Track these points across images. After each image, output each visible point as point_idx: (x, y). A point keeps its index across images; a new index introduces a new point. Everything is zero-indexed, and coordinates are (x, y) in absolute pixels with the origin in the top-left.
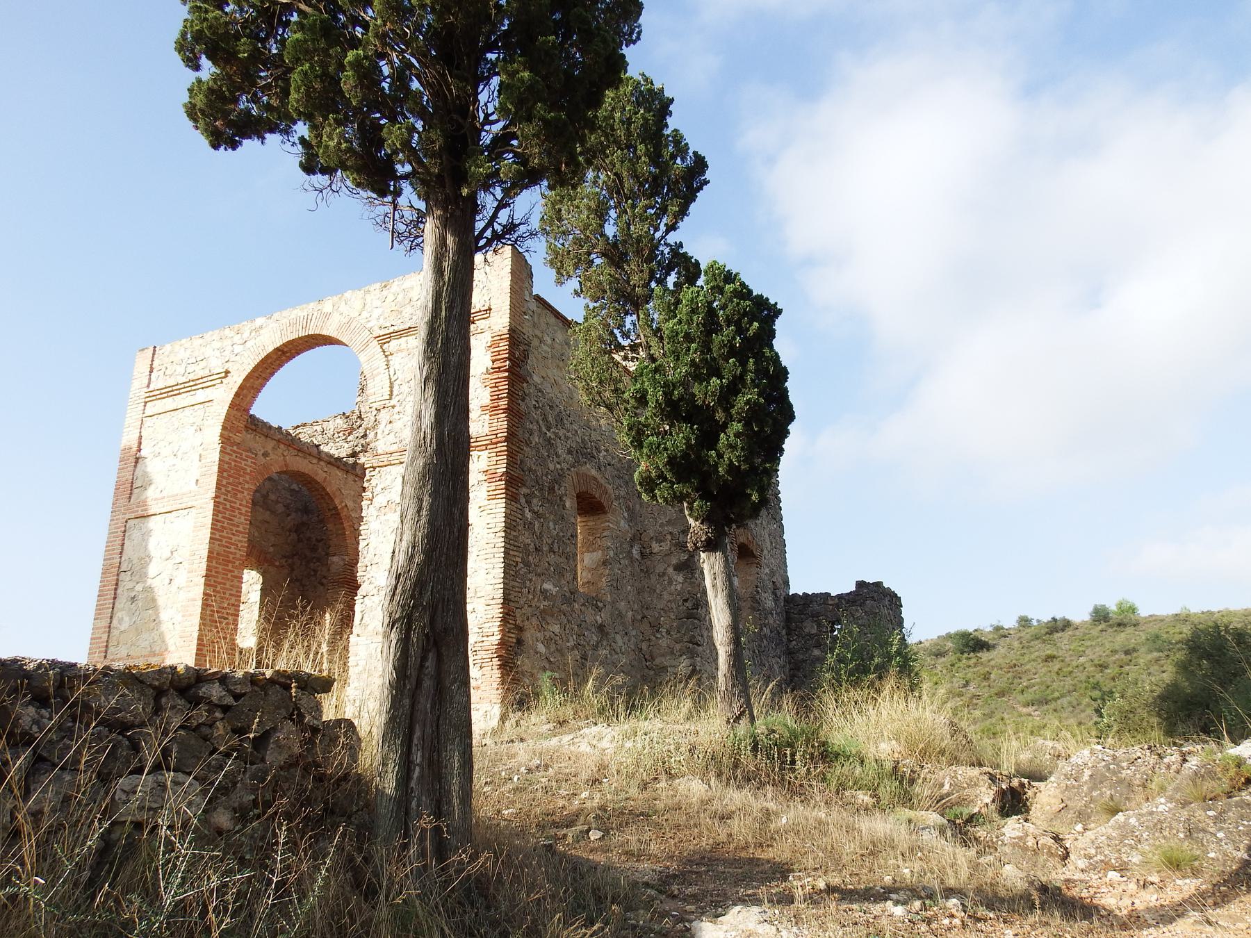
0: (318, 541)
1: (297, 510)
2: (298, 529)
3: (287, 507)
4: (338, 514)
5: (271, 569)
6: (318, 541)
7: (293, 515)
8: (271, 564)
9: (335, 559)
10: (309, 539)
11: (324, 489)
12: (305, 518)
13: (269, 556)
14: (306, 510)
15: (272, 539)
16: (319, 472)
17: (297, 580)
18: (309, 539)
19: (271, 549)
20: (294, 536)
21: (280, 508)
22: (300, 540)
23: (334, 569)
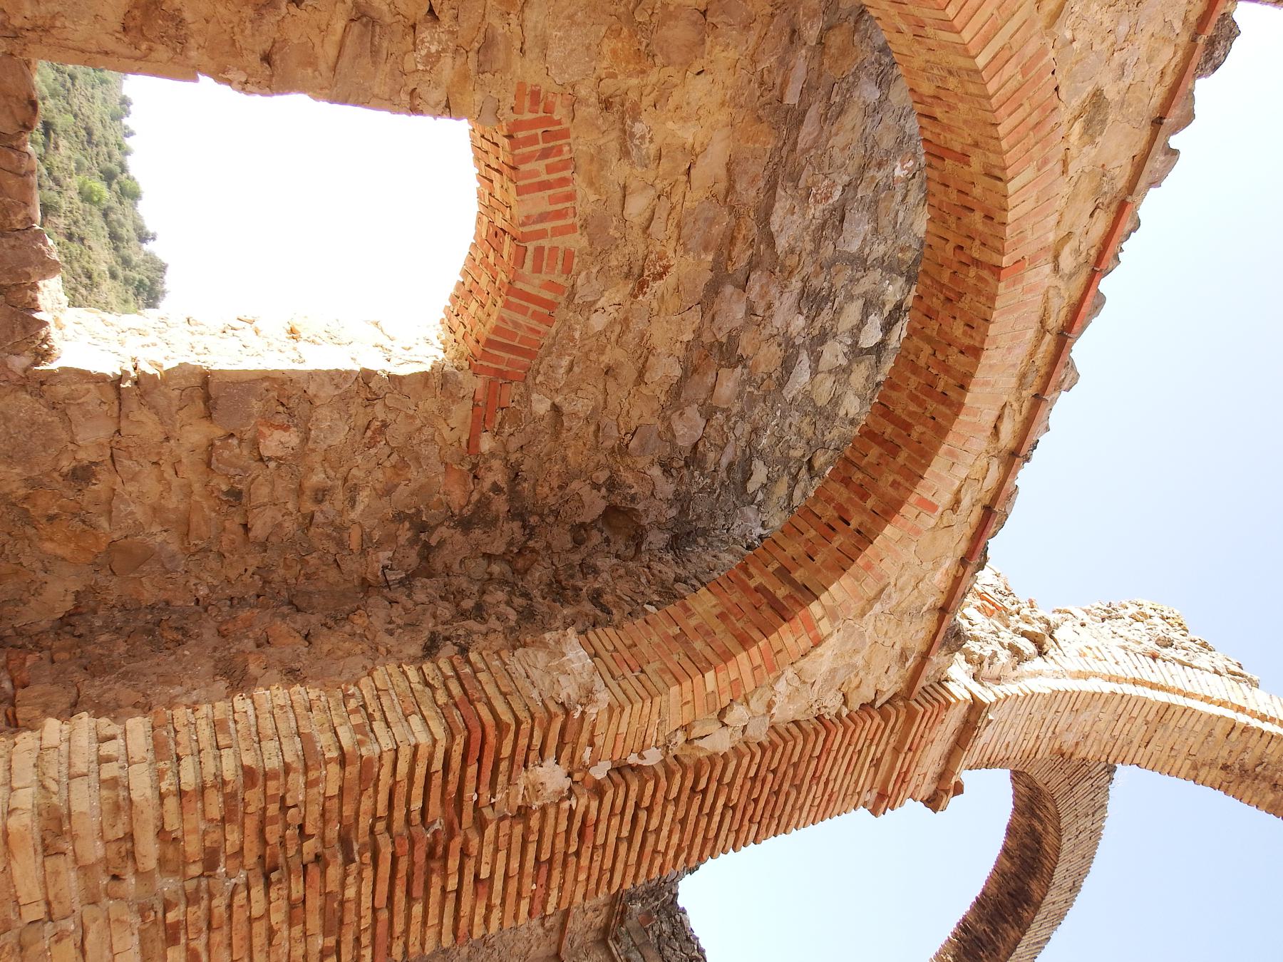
0: (596, 597)
1: (682, 501)
2: (621, 518)
3: (694, 458)
4: (782, 613)
5: (461, 413)
6: (596, 597)
7: (667, 488)
8: (485, 414)
9: (576, 656)
10: (588, 569)
11: (889, 511)
12: (657, 539)
13: (513, 392)
14: (681, 539)
15: (581, 405)
16: (955, 470)
17: (427, 551)
18: (588, 569)
19: (541, 406)
20: (595, 504)
21: (688, 428)
22: (579, 533)
23: (530, 664)
